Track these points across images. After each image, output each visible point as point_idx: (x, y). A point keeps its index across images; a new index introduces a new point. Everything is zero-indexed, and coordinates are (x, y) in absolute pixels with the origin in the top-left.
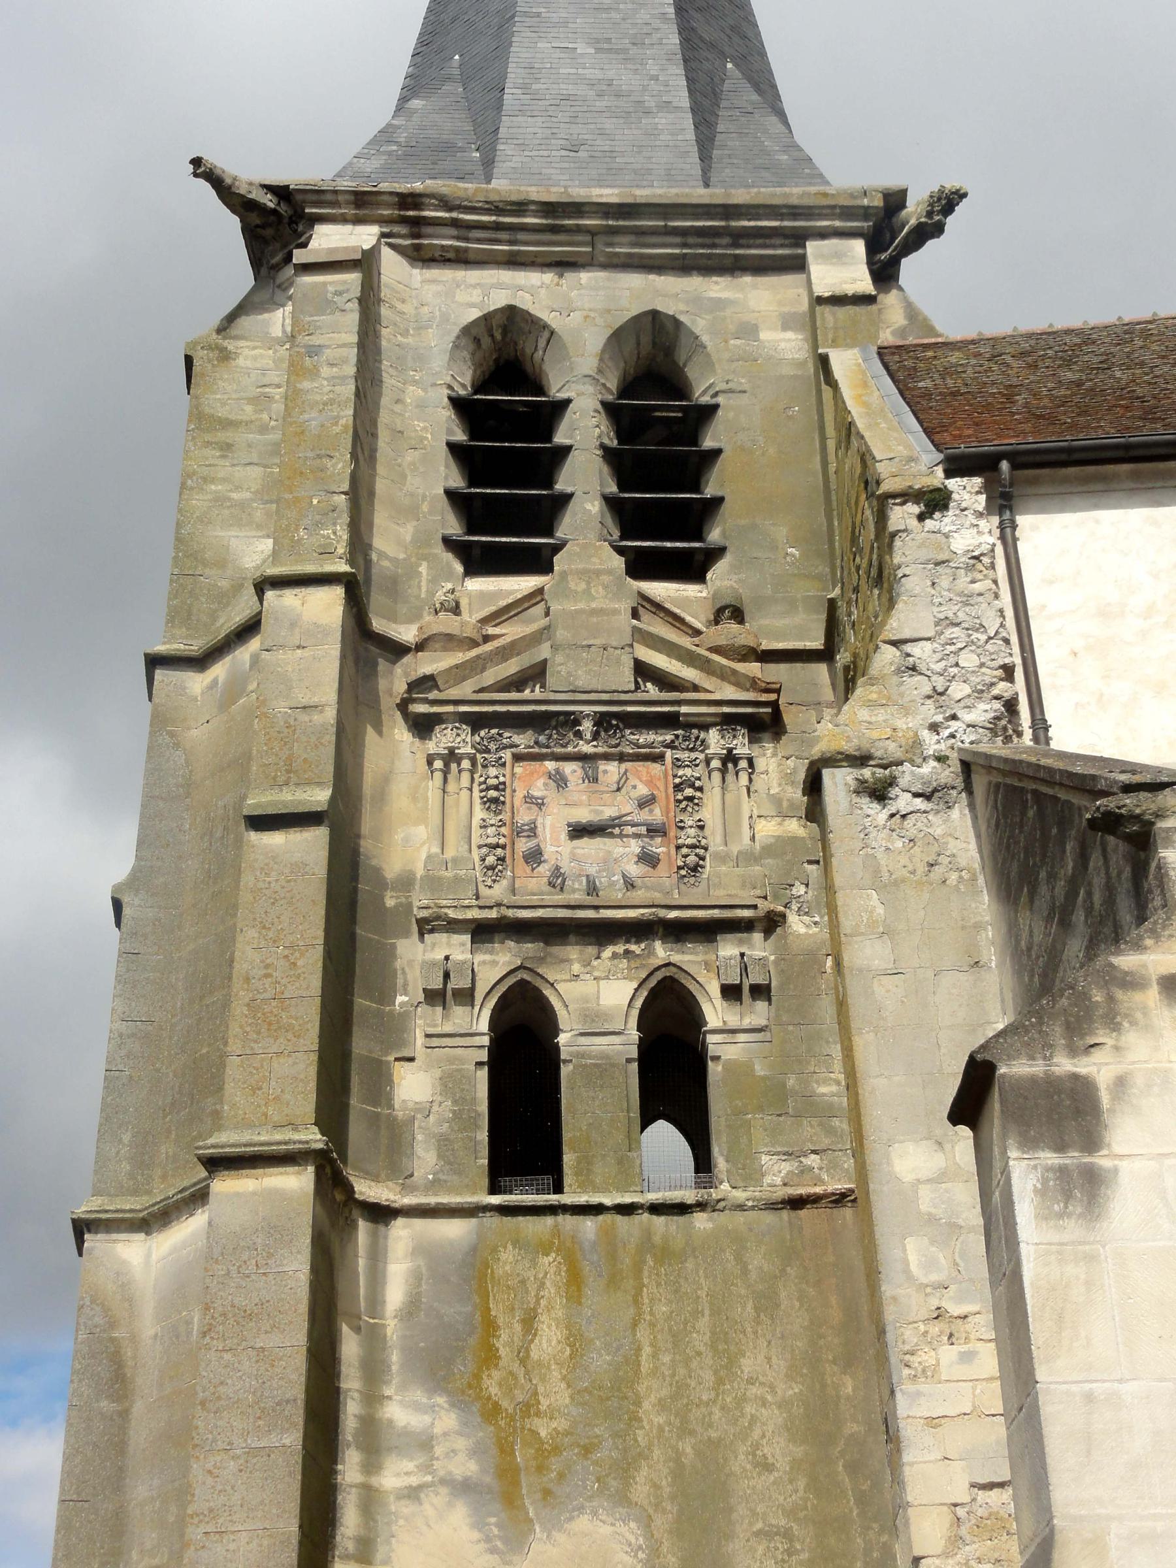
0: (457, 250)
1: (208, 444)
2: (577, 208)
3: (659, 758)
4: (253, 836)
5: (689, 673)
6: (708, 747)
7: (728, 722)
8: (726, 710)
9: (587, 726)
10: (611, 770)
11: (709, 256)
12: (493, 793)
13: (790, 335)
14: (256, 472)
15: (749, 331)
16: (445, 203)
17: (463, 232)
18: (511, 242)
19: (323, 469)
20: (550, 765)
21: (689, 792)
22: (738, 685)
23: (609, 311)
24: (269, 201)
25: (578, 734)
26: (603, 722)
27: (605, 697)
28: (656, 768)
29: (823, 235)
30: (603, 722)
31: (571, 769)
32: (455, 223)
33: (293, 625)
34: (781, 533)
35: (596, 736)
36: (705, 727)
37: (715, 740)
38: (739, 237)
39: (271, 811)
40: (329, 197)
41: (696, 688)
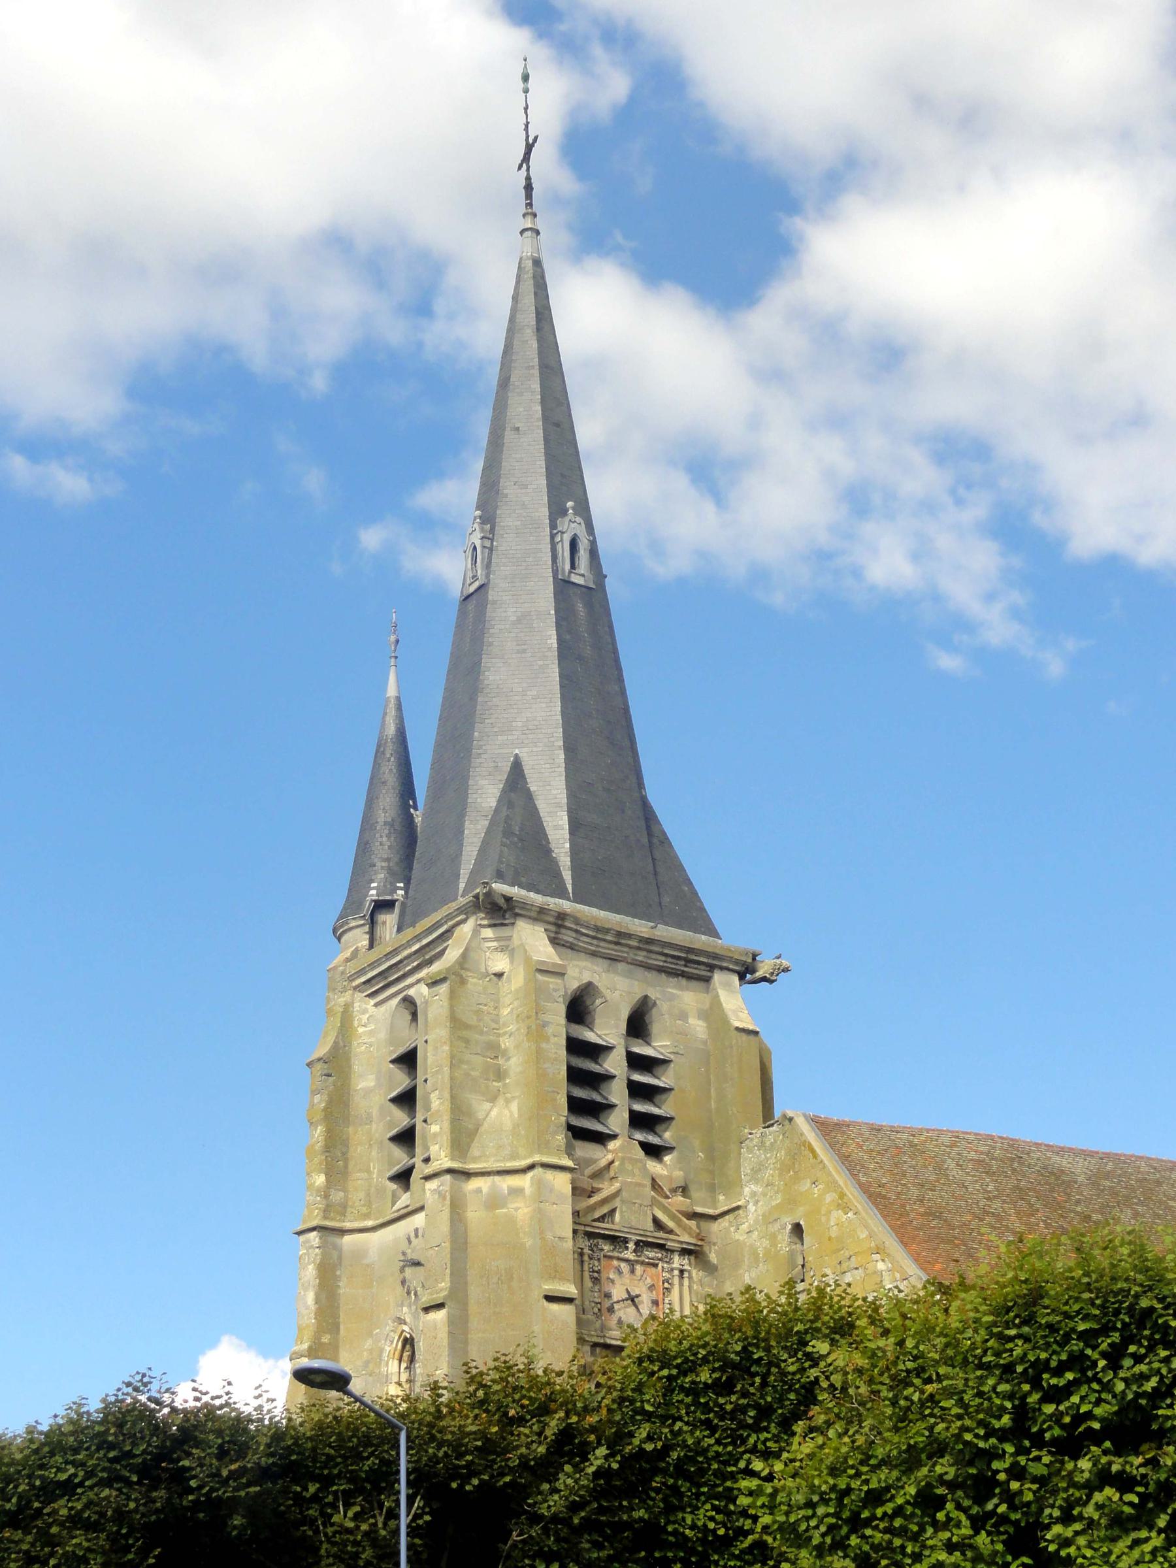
0: (571, 943)
1: (460, 1038)
2: (629, 936)
3: (656, 1265)
4: (546, 1303)
5: (671, 1224)
6: (673, 1263)
7: (685, 1252)
8: (685, 1246)
9: (631, 1246)
10: (638, 1268)
11: (672, 969)
12: (596, 1275)
13: (701, 1023)
14: (479, 1059)
15: (683, 1016)
16: (577, 921)
17: (578, 936)
18: (597, 946)
19: (555, 1100)
20: (615, 1263)
21: (666, 1285)
22: (690, 1235)
23: (630, 993)
24: (501, 902)
25: (627, 1248)
26: (637, 1243)
27: (642, 1233)
28: (653, 1270)
29: (722, 968)
30: (641, 1245)
31: (623, 1265)
32: (577, 931)
33: (551, 1191)
34: (697, 1143)
35: (635, 1251)
36: (672, 1251)
37: (677, 1261)
38: (688, 961)
39: (556, 1295)
40: (528, 907)
41: (671, 1232)
